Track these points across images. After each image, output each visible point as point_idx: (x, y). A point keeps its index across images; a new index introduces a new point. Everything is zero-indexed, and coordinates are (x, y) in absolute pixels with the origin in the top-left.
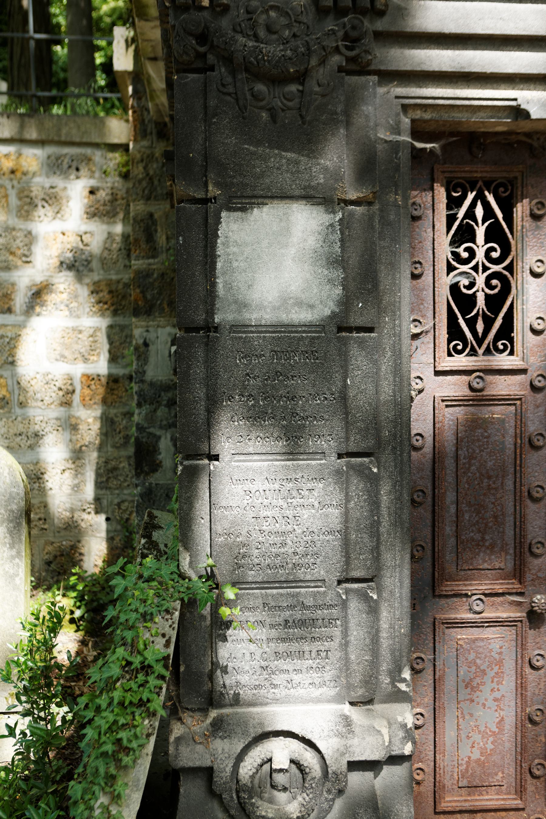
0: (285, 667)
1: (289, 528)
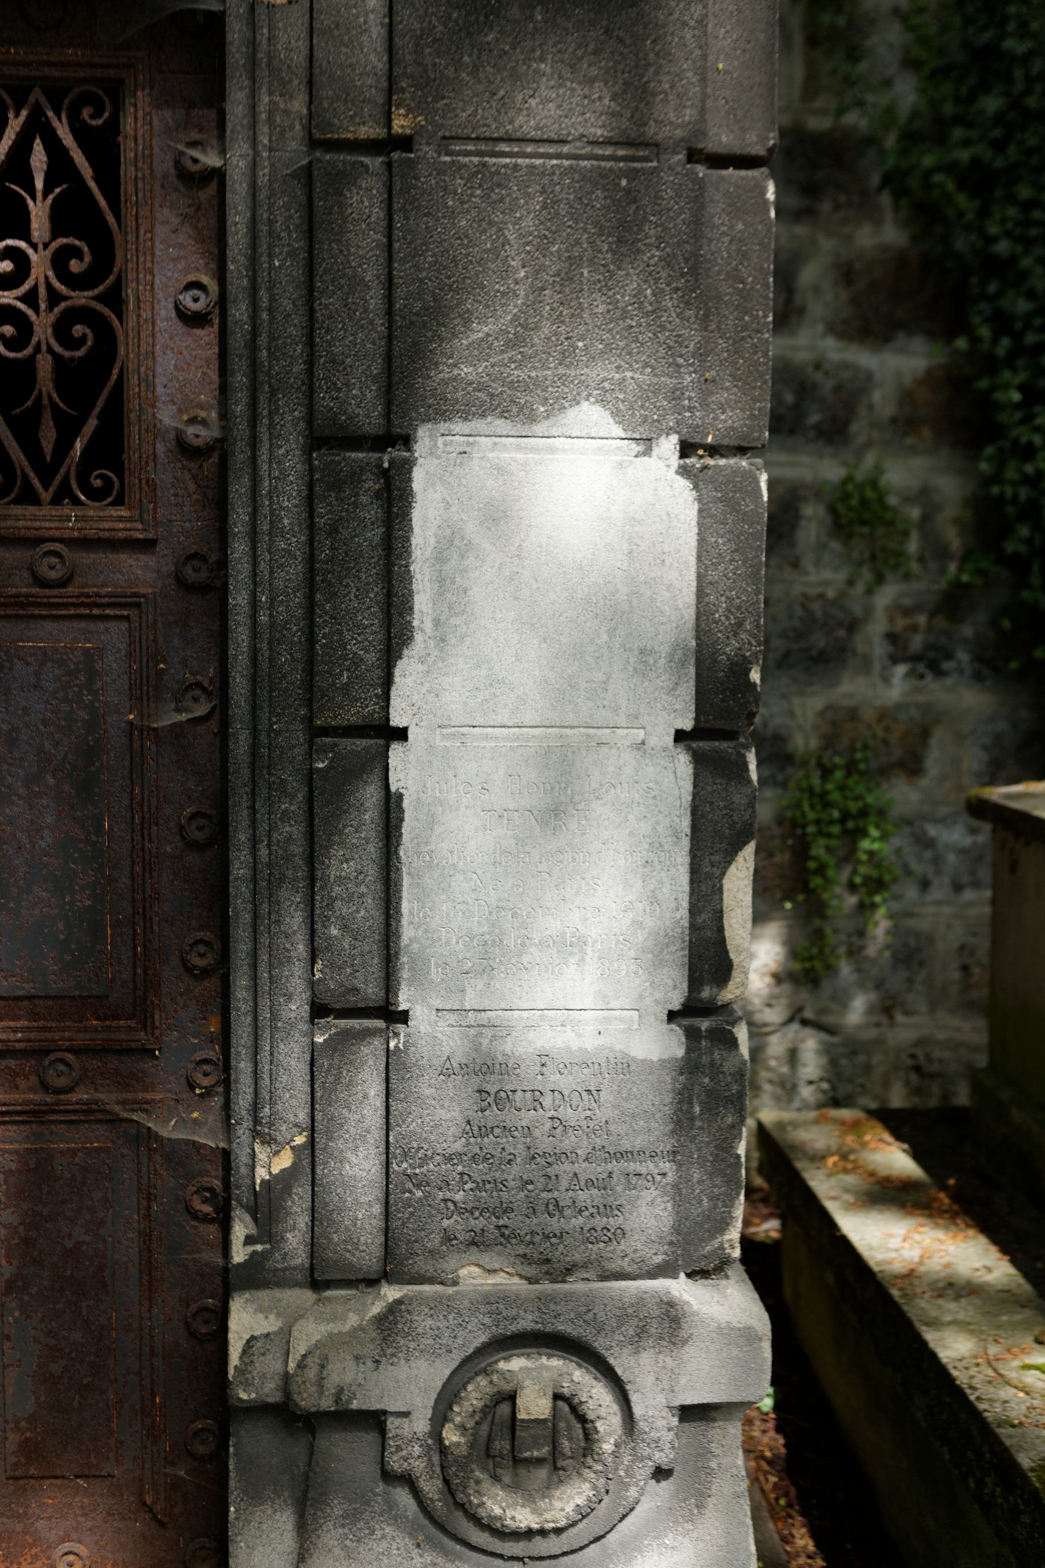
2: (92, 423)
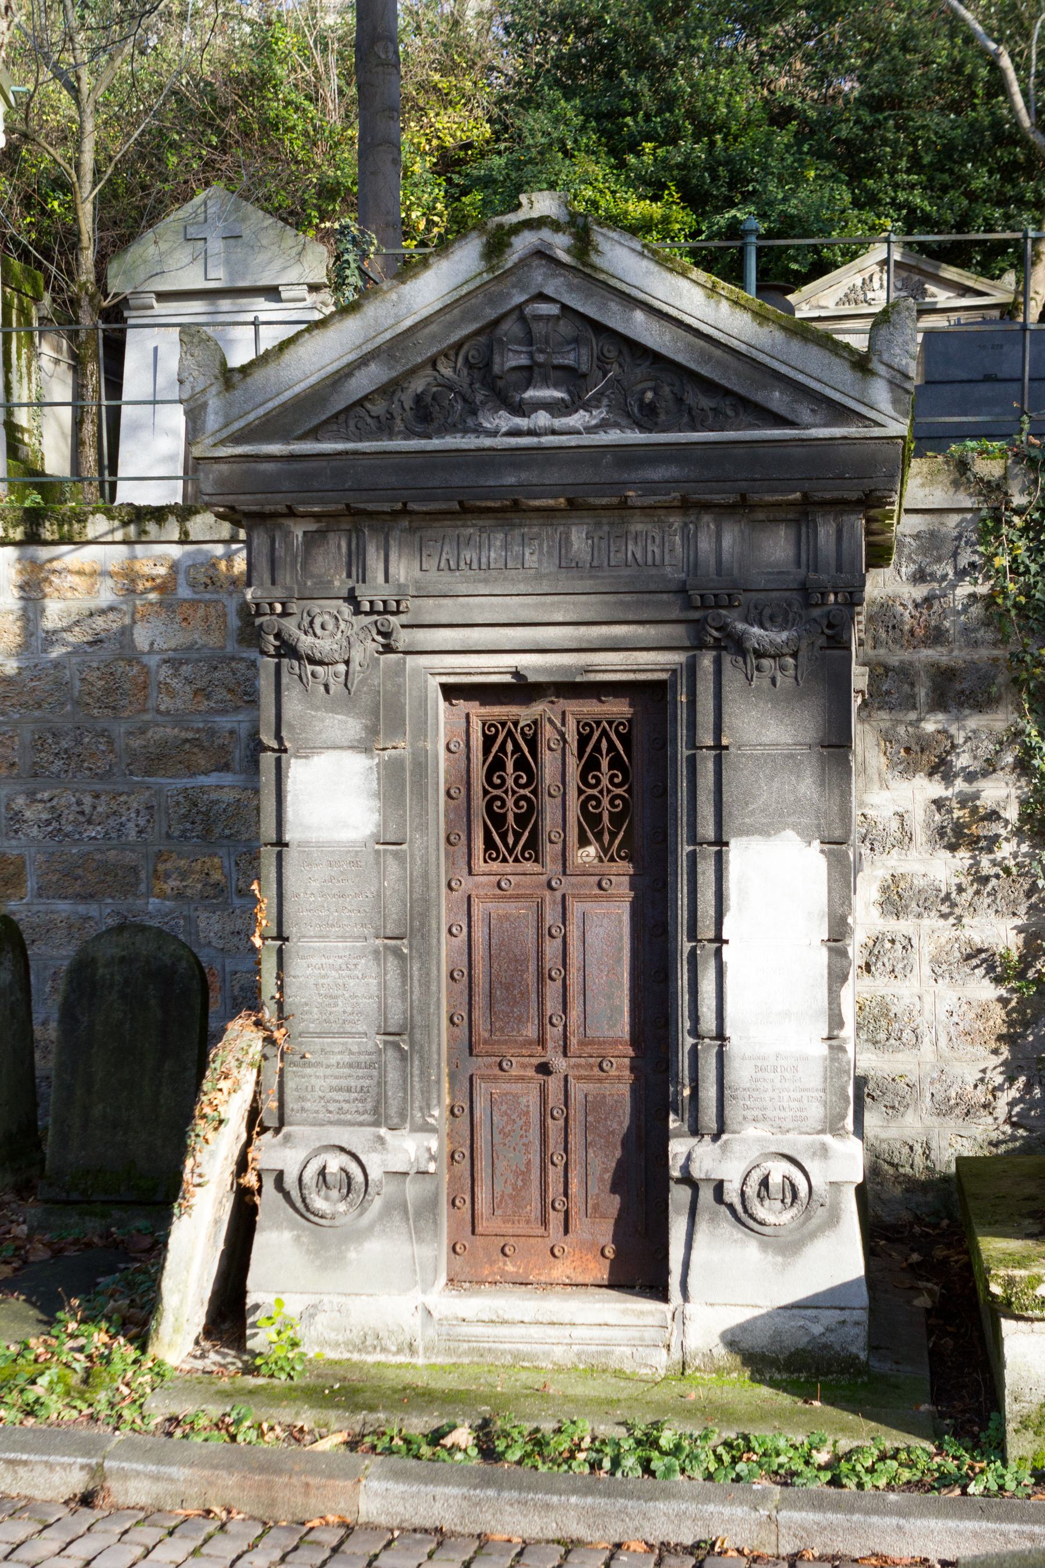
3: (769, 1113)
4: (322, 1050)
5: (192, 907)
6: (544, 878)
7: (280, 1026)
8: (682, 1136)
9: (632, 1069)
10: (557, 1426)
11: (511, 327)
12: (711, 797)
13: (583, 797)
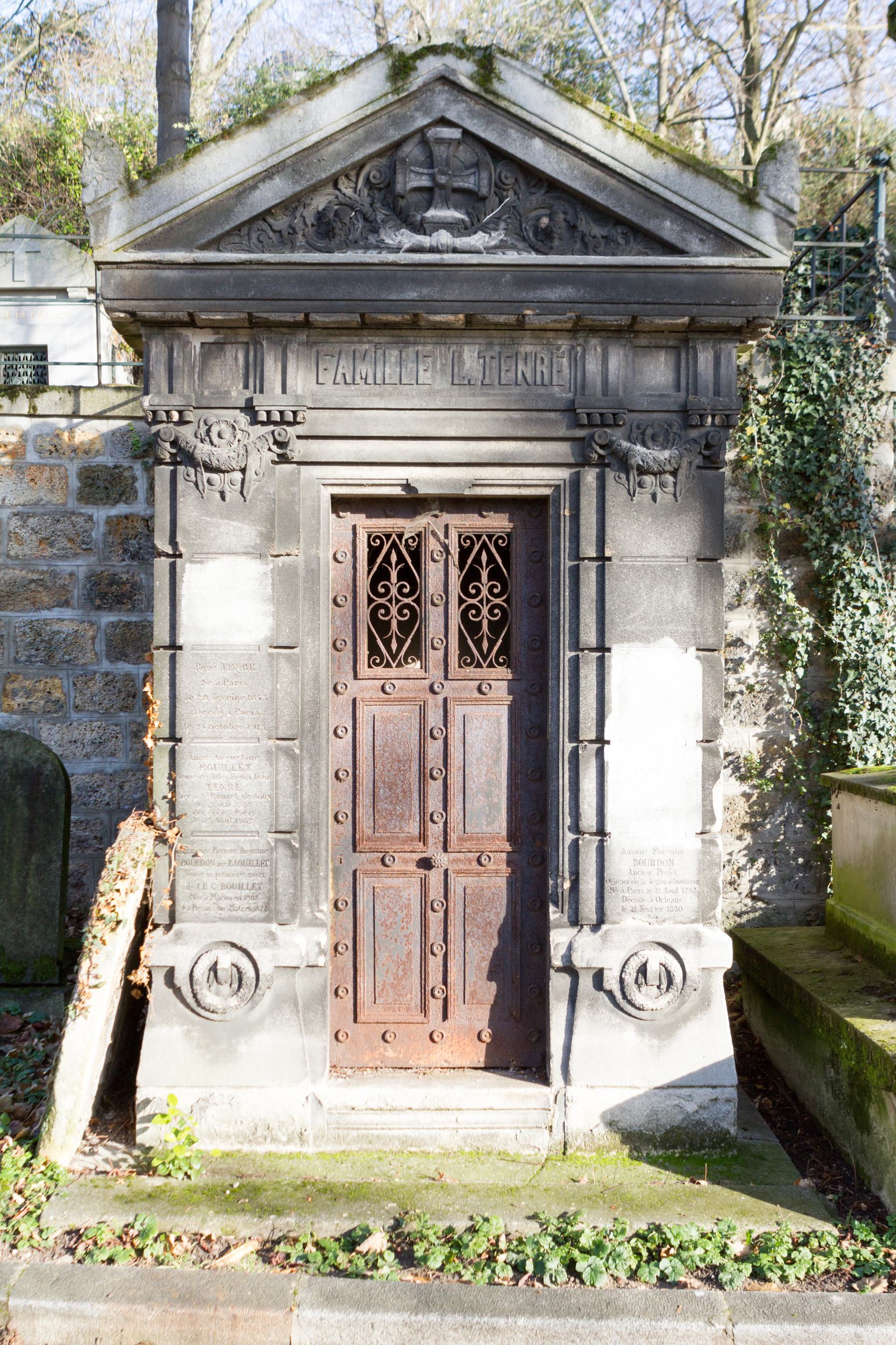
0: (229, 895)
1: (232, 792)
2: (500, 641)
3: (646, 904)
4: (215, 848)
5: (36, 720)
6: (427, 683)
7: (171, 826)
8: (562, 927)
9: (509, 863)
10: (470, 1224)
11: (411, 150)
12: (594, 605)
13: (463, 606)
